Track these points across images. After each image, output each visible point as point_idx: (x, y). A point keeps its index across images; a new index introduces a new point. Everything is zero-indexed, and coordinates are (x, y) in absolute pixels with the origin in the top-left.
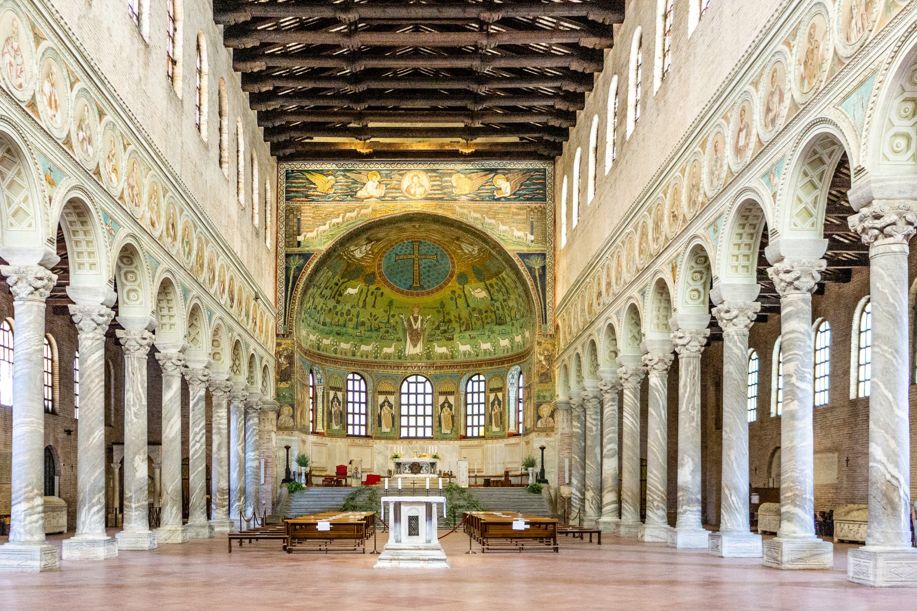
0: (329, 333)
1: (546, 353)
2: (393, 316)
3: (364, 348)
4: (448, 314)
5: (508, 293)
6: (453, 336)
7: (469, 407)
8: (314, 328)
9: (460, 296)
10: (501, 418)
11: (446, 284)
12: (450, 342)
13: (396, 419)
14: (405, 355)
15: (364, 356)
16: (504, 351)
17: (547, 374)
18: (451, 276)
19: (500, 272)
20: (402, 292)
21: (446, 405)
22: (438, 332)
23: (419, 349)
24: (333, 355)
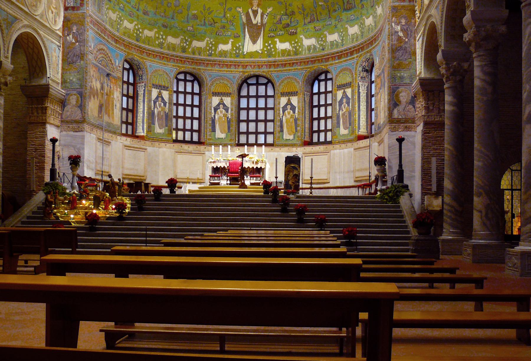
1: (403, 21)
2: (230, 9)
3: (196, 44)
7: (316, 110)
10: (350, 118)
15: (197, 53)
17: (405, 49)
21: (289, 107)
22: (280, 26)
23: (258, 46)
24: (159, 50)
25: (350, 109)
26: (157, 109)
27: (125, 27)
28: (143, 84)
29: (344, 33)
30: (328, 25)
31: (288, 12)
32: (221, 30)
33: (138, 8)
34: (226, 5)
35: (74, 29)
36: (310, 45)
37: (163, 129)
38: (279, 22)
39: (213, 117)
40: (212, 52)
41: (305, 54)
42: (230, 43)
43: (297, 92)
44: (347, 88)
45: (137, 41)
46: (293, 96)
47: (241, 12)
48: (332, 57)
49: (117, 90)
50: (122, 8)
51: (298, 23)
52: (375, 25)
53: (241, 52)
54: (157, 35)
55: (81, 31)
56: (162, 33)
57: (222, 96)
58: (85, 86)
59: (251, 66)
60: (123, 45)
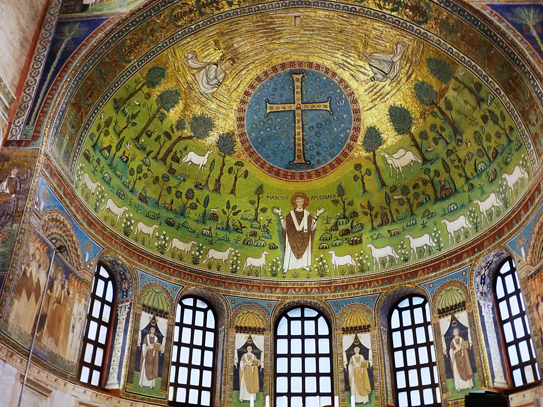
0: (152, 218)
2: (264, 210)
3: (213, 254)
4: (351, 204)
5: (456, 131)
6: (361, 238)
8: (120, 195)
9: (368, 172)
11: (345, 155)
12: (355, 248)
13: (268, 379)
14: (282, 270)
16: (458, 238)
18: (354, 139)
19: (443, 92)
20: (277, 174)
21: (357, 350)
24: (159, 255)
25: (471, 345)
26: (147, 345)
27: (109, 208)
28: (128, 303)
29: (440, 232)
30: (410, 225)
31: (347, 214)
32: (251, 237)
33: (133, 188)
34: (258, 204)
35: (13, 172)
36: (384, 256)
37: (154, 380)
38: (334, 228)
39: (236, 365)
40: (236, 268)
41: (377, 270)
42: (264, 256)
43: (369, 326)
44: (459, 311)
45: (126, 234)
46: (362, 332)
47: (280, 214)
48: (423, 270)
49: (80, 302)
50: (107, 180)
51: (362, 228)
52: (506, 205)
53: (279, 269)
54: (157, 234)
55: (25, 176)
56: (164, 233)
57: (250, 332)
58: (12, 266)
59: (294, 289)
60: (101, 233)
